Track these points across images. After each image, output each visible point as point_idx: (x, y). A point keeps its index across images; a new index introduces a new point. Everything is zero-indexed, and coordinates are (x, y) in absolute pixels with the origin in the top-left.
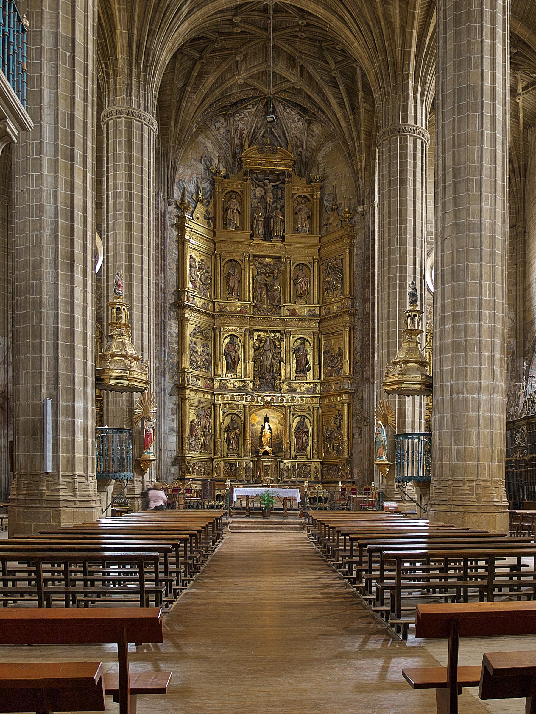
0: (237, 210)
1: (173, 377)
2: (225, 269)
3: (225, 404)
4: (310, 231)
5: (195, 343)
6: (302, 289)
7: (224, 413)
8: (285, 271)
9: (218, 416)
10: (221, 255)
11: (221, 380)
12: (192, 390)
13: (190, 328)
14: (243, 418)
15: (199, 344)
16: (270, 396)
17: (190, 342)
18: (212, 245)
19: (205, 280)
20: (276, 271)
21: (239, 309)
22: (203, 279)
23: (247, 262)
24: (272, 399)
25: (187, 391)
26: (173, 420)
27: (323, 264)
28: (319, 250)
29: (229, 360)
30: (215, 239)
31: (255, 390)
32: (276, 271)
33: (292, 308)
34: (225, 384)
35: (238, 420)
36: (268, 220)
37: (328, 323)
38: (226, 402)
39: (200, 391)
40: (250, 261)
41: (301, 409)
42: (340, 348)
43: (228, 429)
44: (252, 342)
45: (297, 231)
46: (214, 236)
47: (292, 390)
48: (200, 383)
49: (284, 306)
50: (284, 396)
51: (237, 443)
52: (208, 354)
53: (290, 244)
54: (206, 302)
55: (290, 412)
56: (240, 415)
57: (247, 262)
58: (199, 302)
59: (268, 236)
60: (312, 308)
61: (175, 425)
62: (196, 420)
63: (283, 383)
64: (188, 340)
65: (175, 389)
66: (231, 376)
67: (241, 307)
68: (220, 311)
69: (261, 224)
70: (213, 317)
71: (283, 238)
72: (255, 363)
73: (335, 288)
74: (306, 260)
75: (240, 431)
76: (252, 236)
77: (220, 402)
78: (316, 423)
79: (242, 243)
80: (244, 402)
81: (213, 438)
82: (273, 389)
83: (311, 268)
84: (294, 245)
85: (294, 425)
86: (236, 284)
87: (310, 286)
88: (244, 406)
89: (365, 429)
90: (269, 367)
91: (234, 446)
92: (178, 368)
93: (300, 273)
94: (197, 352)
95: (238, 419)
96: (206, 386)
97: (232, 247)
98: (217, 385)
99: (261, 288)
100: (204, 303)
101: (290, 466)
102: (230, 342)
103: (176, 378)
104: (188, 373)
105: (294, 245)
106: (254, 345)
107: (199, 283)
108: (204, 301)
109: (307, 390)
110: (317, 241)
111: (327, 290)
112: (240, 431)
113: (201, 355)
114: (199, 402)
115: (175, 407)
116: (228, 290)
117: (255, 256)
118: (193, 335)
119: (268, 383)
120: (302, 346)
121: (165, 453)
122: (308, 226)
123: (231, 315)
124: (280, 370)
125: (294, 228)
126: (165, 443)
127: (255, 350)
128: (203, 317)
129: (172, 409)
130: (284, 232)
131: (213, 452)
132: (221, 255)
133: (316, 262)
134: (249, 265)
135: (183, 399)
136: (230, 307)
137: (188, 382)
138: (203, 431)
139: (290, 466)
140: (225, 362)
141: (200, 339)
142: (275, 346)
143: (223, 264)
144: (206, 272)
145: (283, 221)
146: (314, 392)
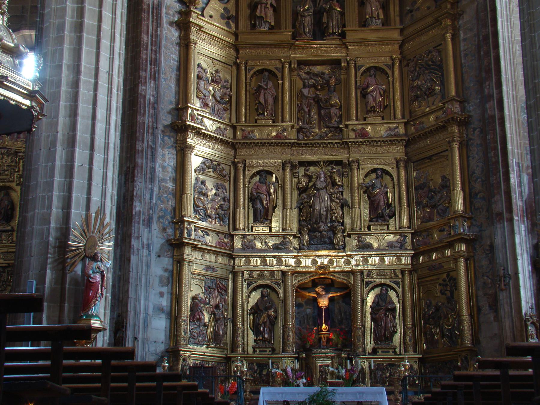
0: (271, 5)
1: (164, 230)
2: (253, 84)
3: (251, 271)
4: (386, 23)
5: (203, 182)
6: (375, 100)
7: (249, 285)
8: (348, 80)
9: (240, 289)
10: (246, 64)
11: (244, 236)
12: (195, 248)
13: (195, 161)
14: (280, 291)
15: (210, 184)
16: (326, 256)
17: (193, 181)
18: (233, 52)
19: (222, 97)
20: (333, 81)
21: (274, 134)
22: (218, 95)
23: (286, 71)
24: (331, 262)
25: (187, 250)
26: (161, 294)
27: (407, 65)
28: (401, 46)
29: (259, 206)
30: (237, 43)
31: (300, 249)
32: (333, 81)
33: (359, 127)
34: (250, 241)
35: (273, 296)
36: (318, 15)
37: (421, 144)
38: (252, 268)
39: (209, 251)
40: (291, 70)
41: (381, 273)
42: (444, 178)
43: (256, 310)
44: (295, 180)
45: (364, 24)
46: (237, 38)
47: (365, 247)
48: (211, 240)
49: (347, 126)
50: (350, 256)
51: (272, 331)
52: (224, 199)
53: (354, 42)
54: (222, 126)
55: (362, 280)
56: (276, 287)
57: (286, 71)
58: (210, 125)
59: (320, 32)
60: (392, 126)
61: (165, 302)
62: (202, 296)
63: (349, 235)
64: (192, 177)
65: (167, 247)
66: (261, 229)
67: (277, 131)
68: (245, 137)
69: (308, 21)
70: (233, 146)
71: (343, 35)
72: (300, 210)
73: (431, 92)
74: (381, 61)
75: (276, 311)
76: (294, 37)
77: (243, 268)
78: (408, 295)
79: (278, 45)
80: (283, 268)
81: (230, 325)
82: (332, 246)
83: (389, 72)
84: (361, 42)
85: (370, 300)
86: (270, 101)
87: (389, 97)
88: (284, 273)
89: (502, 296)
90: (324, 213)
91: (267, 335)
92: (174, 217)
93: (371, 80)
94: (205, 195)
95: (273, 296)
96: (220, 244)
97: (263, 52)
98: (238, 244)
99: (309, 105)
100: (219, 128)
101: (365, 365)
102: (260, 181)
103: (170, 231)
104: (190, 223)
105: (361, 42)
106: (299, 182)
107: (211, 102)
108: (218, 125)
109: (391, 245)
110: (396, 35)
111: (416, 98)
112: (276, 311)
113: (213, 200)
114: (208, 268)
115: (166, 274)
116: (257, 110)
117: (301, 63)
118: (200, 170)
119: (322, 237)
120: (378, 181)
121: (144, 344)
122: (382, 16)
123: (262, 144)
124: (343, 217)
125: (360, 22)
126: (145, 328)
127: (302, 191)
128: (218, 146)
129: (161, 277)
130: (344, 26)
131: (229, 347)
132: (246, 64)
133: (397, 63)
134: (290, 76)
135: (180, 262)
136: (261, 132)
137: (189, 235)
138: (213, 314)
139: (365, 365)
140: (251, 211)
141: (212, 177)
142: (334, 184)
143: (249, 75)
144: (224, 87)
145: (342, 14)
146: (402, 246)
